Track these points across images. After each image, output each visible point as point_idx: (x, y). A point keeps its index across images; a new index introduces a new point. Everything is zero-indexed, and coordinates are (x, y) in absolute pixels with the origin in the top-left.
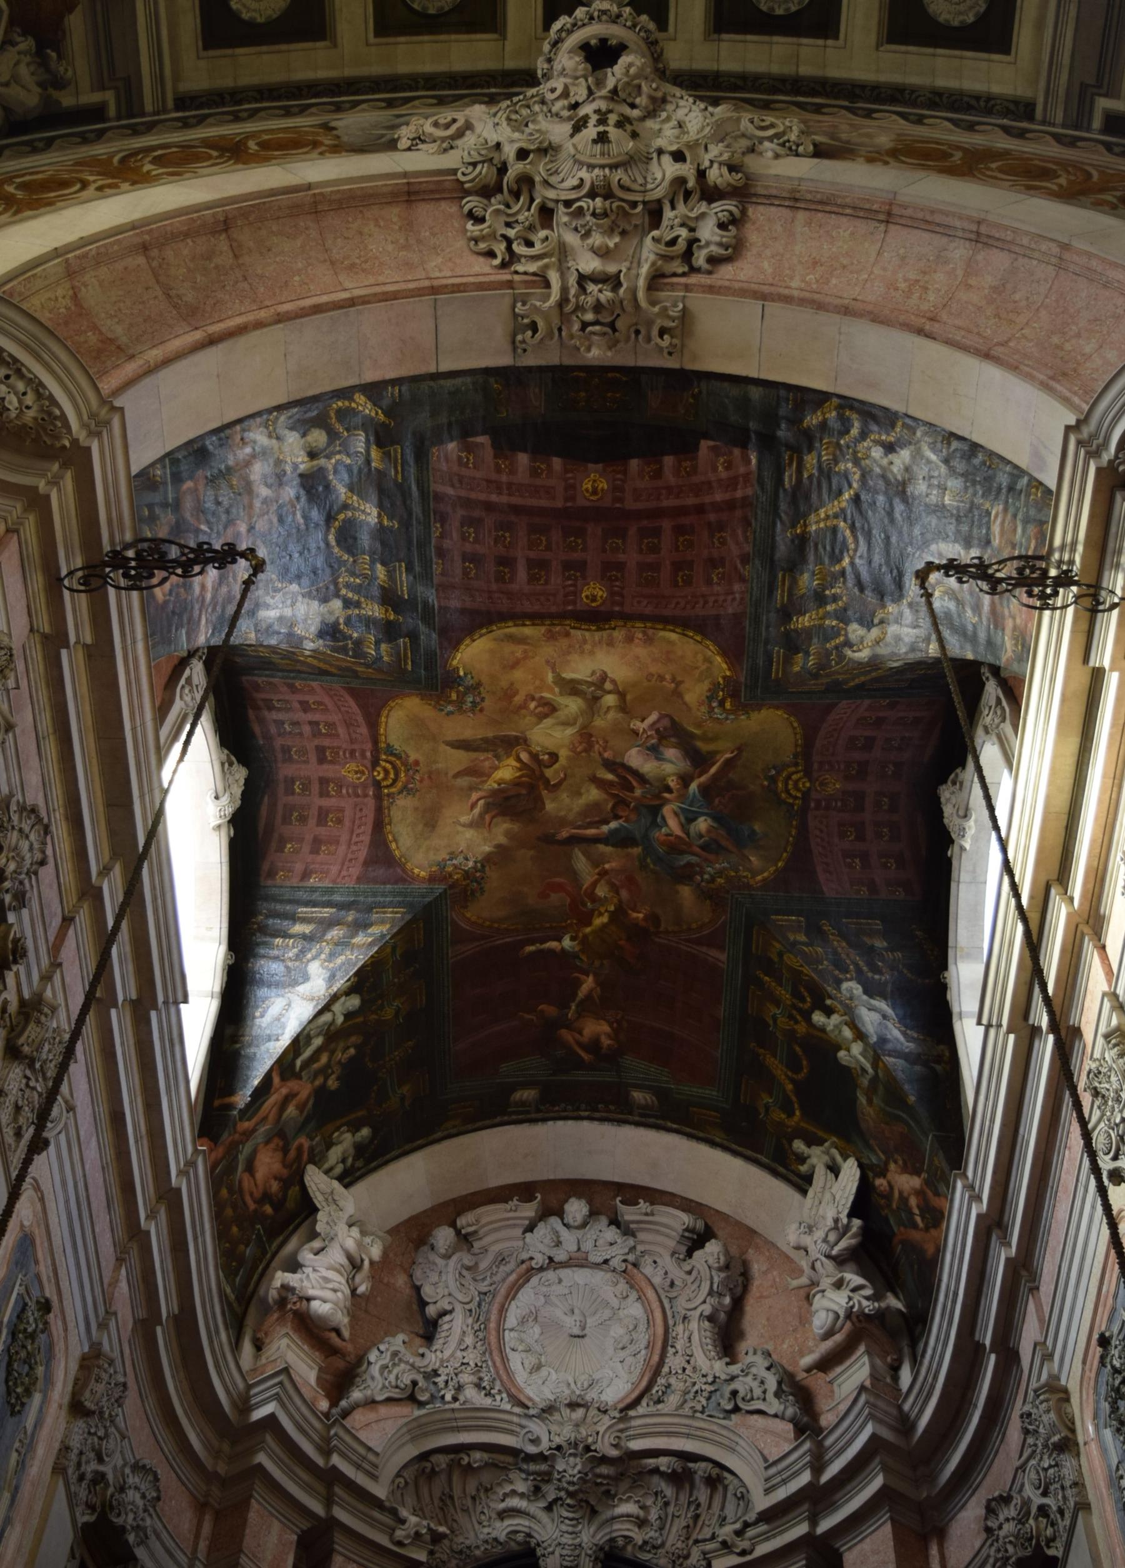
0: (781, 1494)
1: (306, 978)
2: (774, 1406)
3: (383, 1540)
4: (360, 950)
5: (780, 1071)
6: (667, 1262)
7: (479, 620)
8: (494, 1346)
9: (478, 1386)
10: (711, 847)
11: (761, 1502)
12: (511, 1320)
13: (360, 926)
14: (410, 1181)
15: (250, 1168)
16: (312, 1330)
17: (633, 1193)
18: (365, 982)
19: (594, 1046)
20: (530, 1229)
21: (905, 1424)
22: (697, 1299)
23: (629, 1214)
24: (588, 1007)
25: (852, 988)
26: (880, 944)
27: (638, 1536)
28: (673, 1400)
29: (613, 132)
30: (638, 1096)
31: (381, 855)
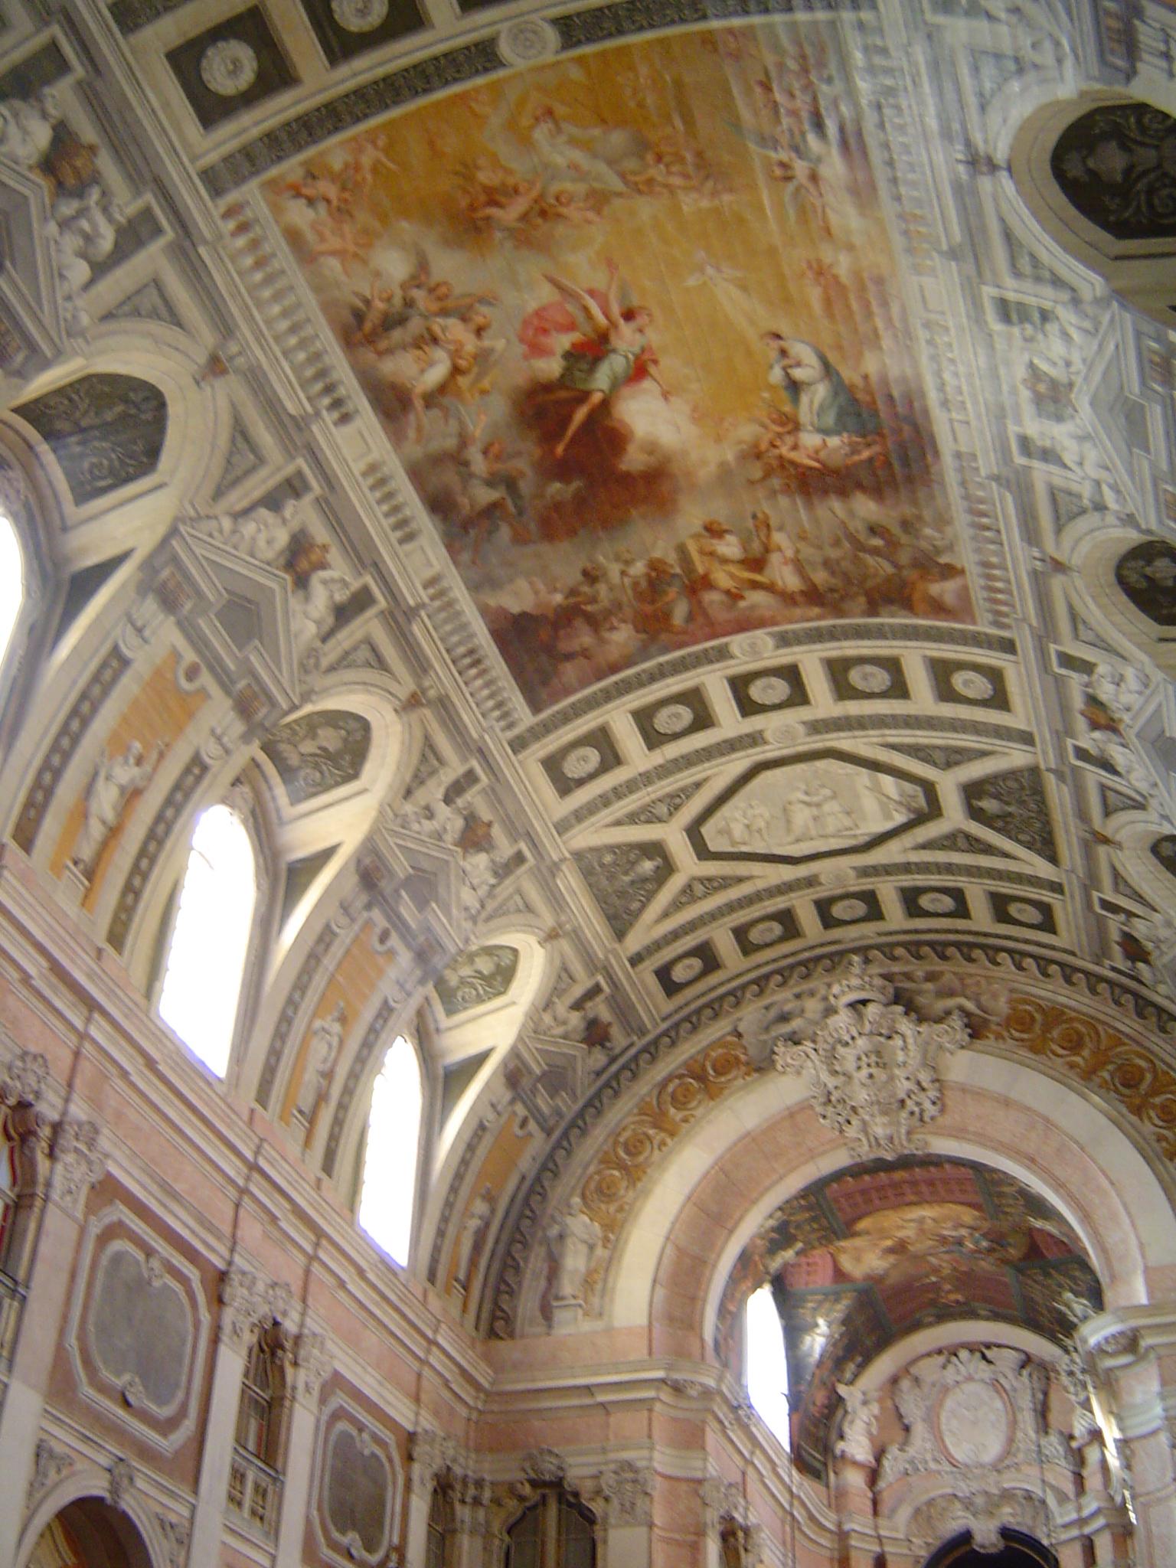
0: (1067, 1519)
1: (817, 1325)
2: (1063, 1462)
3: (905, 1551)
4: (840, 1309)
5: (1045, 1312)
6: (1010, 1375)
7: (860, 1218)
8: (939, 1438)
9: (935, 1460)
10: (990, 1251)
11: (1060, 1521)
12: (943, 1419)
13: (837, 1301)
14: (884, 1365)
15: (814, 1404)
16: (856, 1464)
17: (988, 1346)
18: (844, 1322)
19: (957, 1302)
20: (944, 1367)
21: (1111, 1498)
22: (1026, 1402)
23: (987, 1353)
24: (950, 1292)
25: (1068, 1295)
26: (1077, 1274)
27: (1011, 1519)
28: (1021, 1456)
29: (873, 1070)
30: (983, 1313)
31: (839, 1275)
